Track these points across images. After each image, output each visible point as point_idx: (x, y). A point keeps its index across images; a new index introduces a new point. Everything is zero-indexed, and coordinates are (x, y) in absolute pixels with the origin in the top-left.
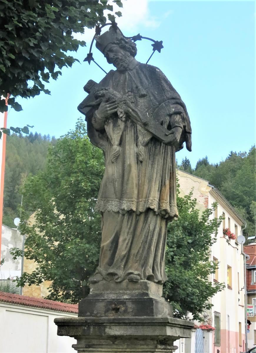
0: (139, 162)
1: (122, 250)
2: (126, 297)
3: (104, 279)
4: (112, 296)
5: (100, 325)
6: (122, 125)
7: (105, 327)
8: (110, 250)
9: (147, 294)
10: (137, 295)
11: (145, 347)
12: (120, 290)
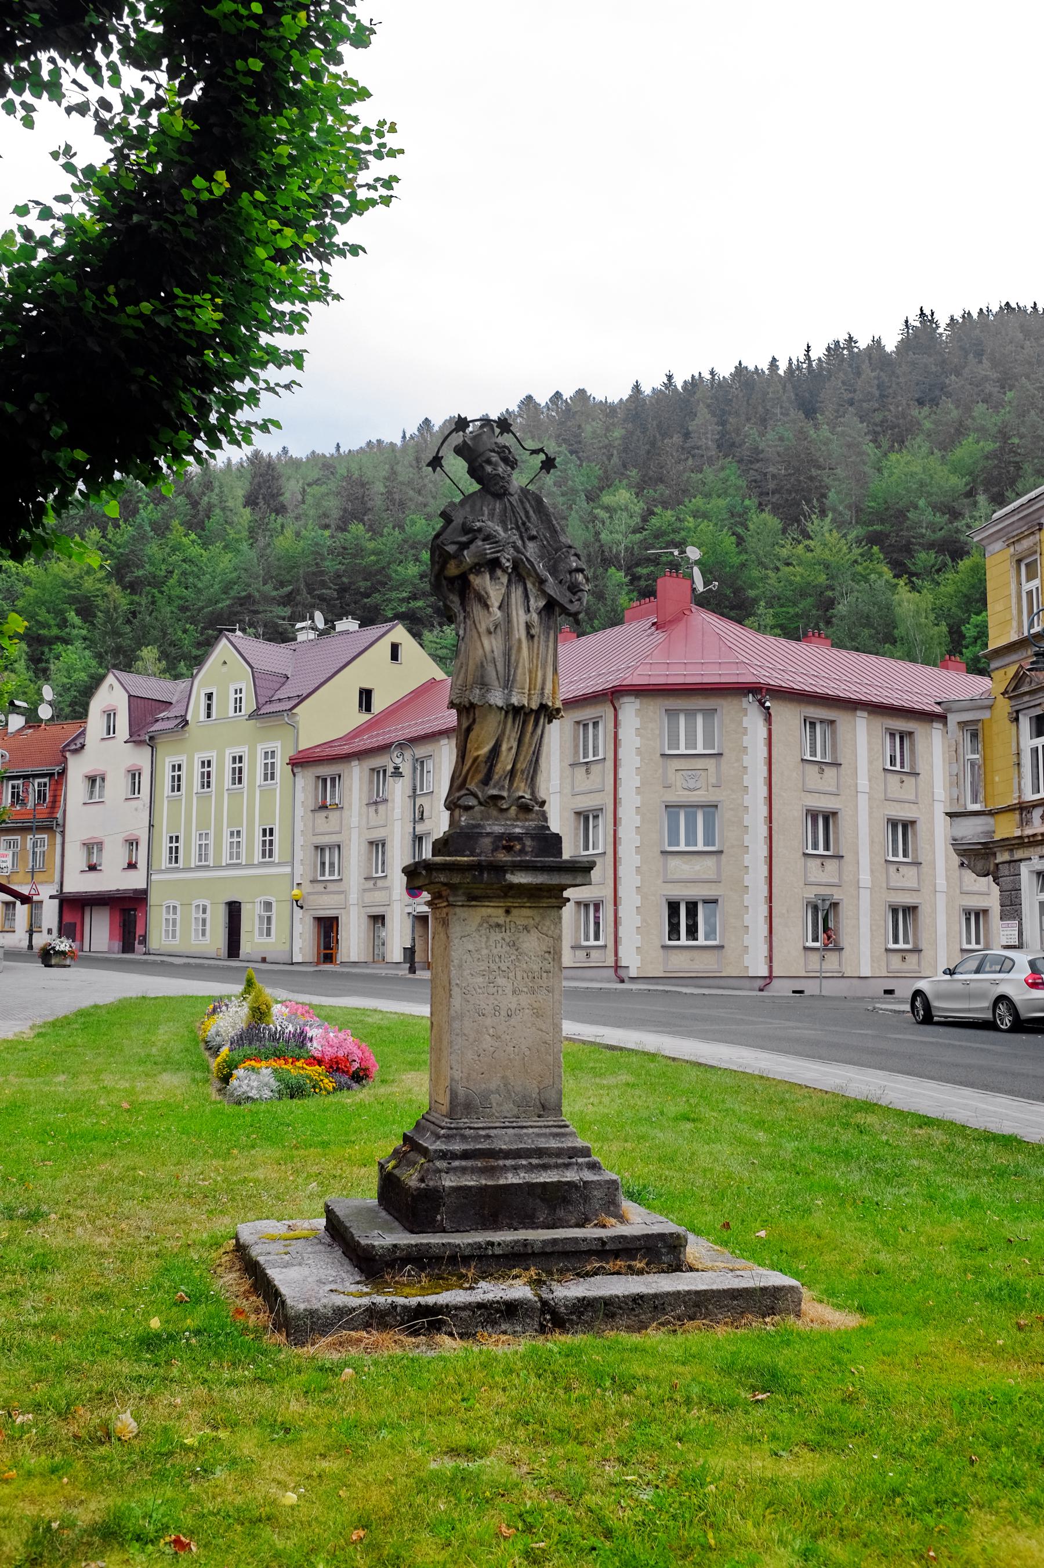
0: (531, 637)
1: (505, 762)
2: (518, 830)
3: (480, 804)
4: (498, 829)
5: (499, 869)
6: (505, 580)
7: (505, 872)
8: (486, 762)
9: (548, 828)
10: (534, 829)
11: (554, 900)
12: (507, 819)
